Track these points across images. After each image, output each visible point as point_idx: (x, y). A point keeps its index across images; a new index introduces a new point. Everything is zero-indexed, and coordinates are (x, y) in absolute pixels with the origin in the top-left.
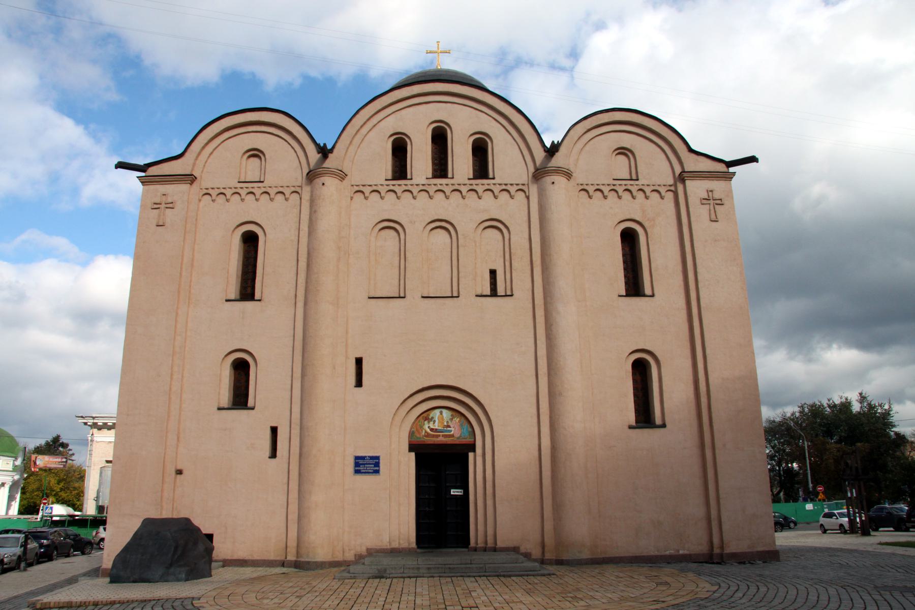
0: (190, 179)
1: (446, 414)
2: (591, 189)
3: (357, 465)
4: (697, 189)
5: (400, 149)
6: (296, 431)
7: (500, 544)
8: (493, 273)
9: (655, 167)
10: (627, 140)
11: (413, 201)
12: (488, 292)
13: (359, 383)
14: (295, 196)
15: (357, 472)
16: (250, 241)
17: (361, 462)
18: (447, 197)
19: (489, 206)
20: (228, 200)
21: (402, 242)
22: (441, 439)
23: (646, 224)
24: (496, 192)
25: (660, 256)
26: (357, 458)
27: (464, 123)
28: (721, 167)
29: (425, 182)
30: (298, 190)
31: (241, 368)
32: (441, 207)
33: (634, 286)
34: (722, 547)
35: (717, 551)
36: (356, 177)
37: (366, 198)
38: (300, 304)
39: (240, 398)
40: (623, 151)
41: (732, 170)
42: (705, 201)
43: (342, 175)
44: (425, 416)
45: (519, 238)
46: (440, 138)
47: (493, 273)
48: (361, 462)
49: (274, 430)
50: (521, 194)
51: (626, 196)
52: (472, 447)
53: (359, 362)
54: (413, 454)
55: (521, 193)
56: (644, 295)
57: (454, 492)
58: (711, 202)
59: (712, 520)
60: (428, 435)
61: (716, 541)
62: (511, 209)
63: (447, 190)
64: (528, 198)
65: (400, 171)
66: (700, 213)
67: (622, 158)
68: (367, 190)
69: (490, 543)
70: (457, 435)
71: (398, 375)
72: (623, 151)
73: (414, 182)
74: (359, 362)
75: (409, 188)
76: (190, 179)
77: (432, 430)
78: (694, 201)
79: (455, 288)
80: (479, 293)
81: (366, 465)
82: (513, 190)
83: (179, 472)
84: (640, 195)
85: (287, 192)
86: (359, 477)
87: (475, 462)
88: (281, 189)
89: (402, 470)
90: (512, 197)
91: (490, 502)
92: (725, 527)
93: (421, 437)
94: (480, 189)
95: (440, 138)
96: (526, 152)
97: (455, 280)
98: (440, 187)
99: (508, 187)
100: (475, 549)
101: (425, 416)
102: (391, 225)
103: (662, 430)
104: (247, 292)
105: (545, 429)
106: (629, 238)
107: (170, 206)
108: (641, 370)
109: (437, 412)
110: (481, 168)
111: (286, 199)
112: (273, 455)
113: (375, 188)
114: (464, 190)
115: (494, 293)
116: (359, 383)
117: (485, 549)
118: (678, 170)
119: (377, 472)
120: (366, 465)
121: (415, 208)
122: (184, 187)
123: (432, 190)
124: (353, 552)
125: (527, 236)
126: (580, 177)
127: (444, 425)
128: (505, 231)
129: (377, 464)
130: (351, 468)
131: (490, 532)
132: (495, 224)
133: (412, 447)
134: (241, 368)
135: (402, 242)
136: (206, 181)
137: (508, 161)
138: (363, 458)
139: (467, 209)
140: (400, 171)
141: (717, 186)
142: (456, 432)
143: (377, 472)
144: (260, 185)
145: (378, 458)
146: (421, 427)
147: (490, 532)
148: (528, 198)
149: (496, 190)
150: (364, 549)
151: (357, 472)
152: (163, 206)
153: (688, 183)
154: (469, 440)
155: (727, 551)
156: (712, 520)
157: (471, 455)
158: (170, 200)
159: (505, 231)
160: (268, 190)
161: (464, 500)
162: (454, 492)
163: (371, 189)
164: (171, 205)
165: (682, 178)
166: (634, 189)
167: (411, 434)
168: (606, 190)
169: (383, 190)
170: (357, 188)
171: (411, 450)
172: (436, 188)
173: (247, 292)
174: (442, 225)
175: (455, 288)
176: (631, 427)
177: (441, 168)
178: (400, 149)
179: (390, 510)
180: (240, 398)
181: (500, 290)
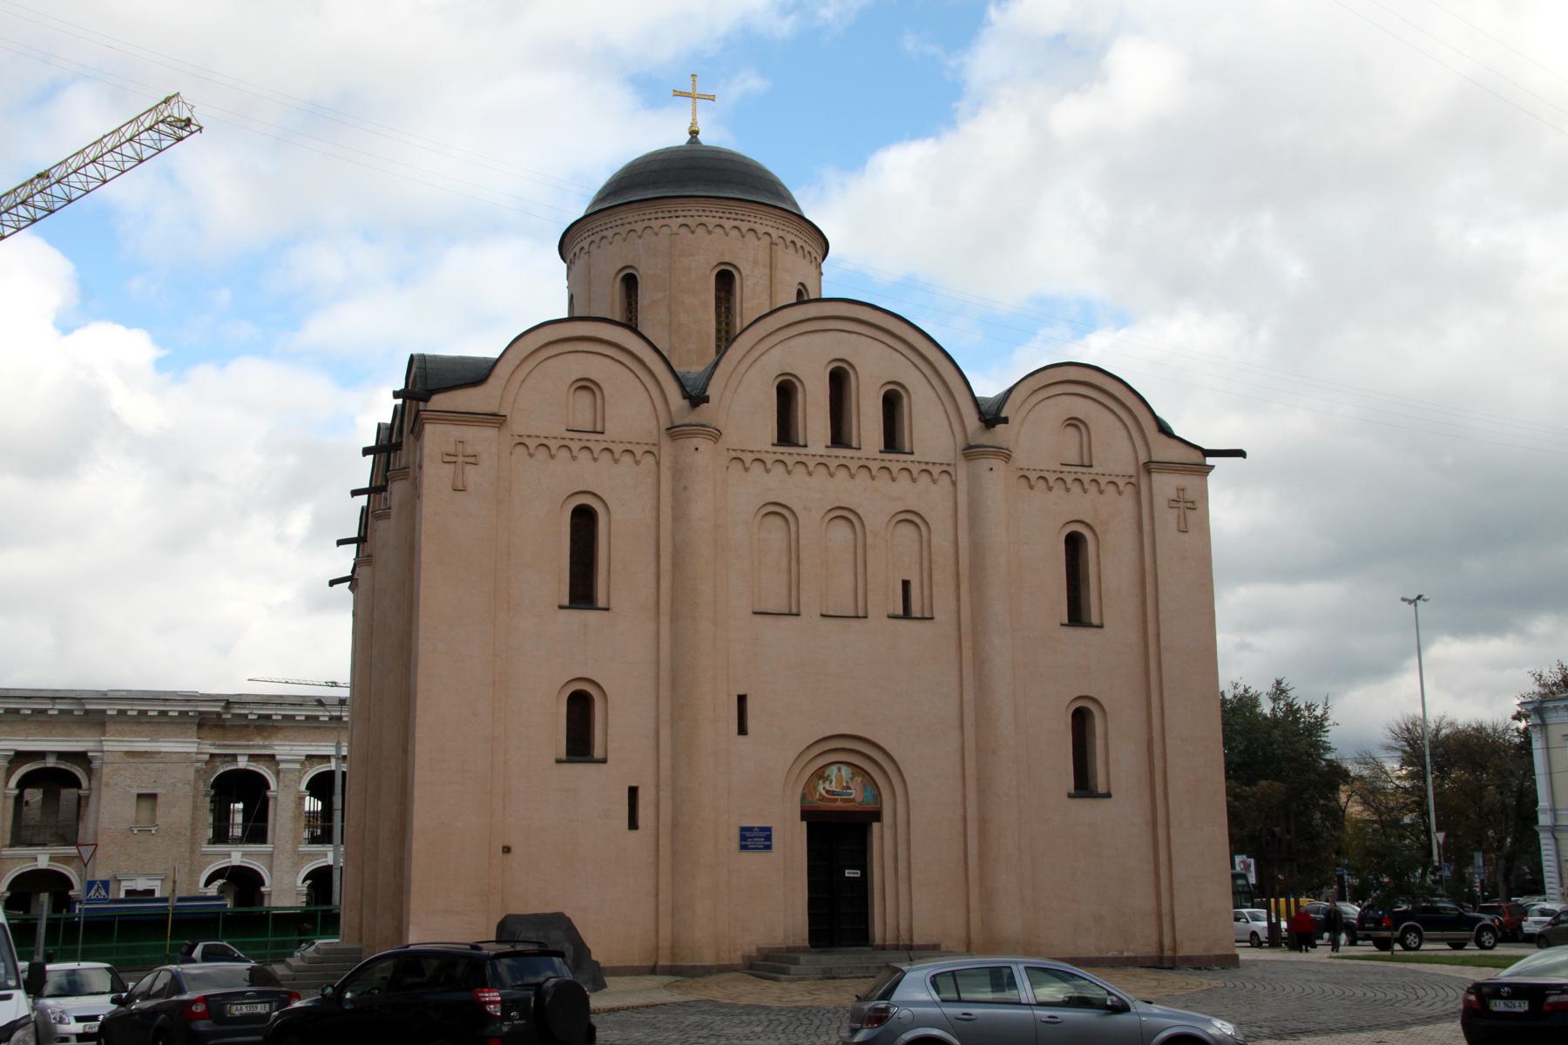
0: (496, 419)
1: (846, 772)
2: (1033, 476)
3: (743, 838)
4: (1165, 485)
5: (786, 392)
6: (665, 794)
7: (917, 941)
8: (906, 584)
9: (1115, 451)
10: (1081, 408)
11: (808, 478)
12: (900, 611)
13: (742, 730)
14: (650, 458)
15: (744, 847)
16: (584, 521)
17: (748, 834)
18: (852, 476)
19: (906, 493)
20: (552, 457)
21: (793, 536)
22: (839, 805)
23: (1097, 530)
24: (915, 473)
25: (1112, 572)
26: (743, 829)
27: (874, 368)
28: (1195, 457)
29: (823, 451)
30: (654, 449)
31: (580, 707)
33: (1077, 615)
34: (1174, 949)
35: (1167, 953)
36: (732, 438)
37: (746, 470)
38: (665, 619)
39: (580, 744)
40: (1074, 423)
41: (1210, 461)
42: (1173, 502)
43: (716, 435)
44: (820, 775)
45: (941, 540)
47: (906, 584)
48: (748, 834)
49: (633, 792)
50: (945, 477)
51: (1076, 488)
52: (876, 815)
53: (742, 699)
54: (802, 828)
55: (945, 476)
56: (1090, 625)
57: (848, 873)
58: (1181, 505)
59: (1163, 916)
60: (823, 799)
61: (1167, 941)
62: (932, 499)
63: (853, 465)
64: (954, 483)
66: (1167, 519)
67: (1071, 430)
68: (748, 458)
69: (904, 940)
70: (859, 800)
72: (1074, 423)
73: (811, 450)
74: (742, 699)
75: (804, 459)
76: (496, 419)
77: (828, 792)
78: (1160, 502)
79: (861, 604)
80: (891, 612)
81: (755, 839)
82: (936, 471)
83: (507, 850)
84: (1093, 488)
85: (638, 451)
86: (746, 855)
87: (880, 835)
88: (629, 447)
90: (934, 481)
91: (903, 887)
92: (1178, 924)
93: (815, 802)
94: (895, 467)
96: (954, 418)
97: (860, 593)
98: (843, 462)
99: (930, 467)
100: (883, 948)
101: (820, 775)
102: (778, 511)
103: (1106, 801)
105: (972, 796)
106: (1074, 544)
107: (473, 459)
108: (1081, 720)
109: (834, 768)
111: (637, 463)
112: (633, 824)
113: (758, 456)
114: (874, 466)
115: (907, 614)
117: (897, 948)
118: (1143, 458)
119: (768, 847)
120: (755, 839)
121: (811, 488)
122: (489, 433)
123: (833, 463)
124: (739, 953)
125: (951, 537)
126: (1021, 458)
128: (918, 521)
129: (769, 838)
130: (736, 843)
131: (903, 925)
132: (911, 518)
133: (806, 815)
134: (580, 707)
135: (793, 536)
136: (518, 425)
137: (930, 429)
138: (750, 829)
139: (877, 495)
140: (786, 434)
141: (1187, 481)
142: (858, 795)
143: (768, 847)
144: (598, 437)
145: (769, 829)
146: (815, 788)
147: (903, 925)
148: (954, 483)
149: (915, 469)
150: (754, 948)
151: (744, 847)
152: (460, 459)
153: (1155, 476)
154: (871, 807)
155: (1181, 953)
156: (1163, 916)
157: (876, 826)
158: (470, 451)
159: (918, 521)
160: (612, 446)
161: (863, 885)
162: (848, 873)
163: (754, 456)
164: (472, 460)
165: (1149, 467)
166: (1086, 479)
167: (803, 797)
168: (1051, 478)
169: (769, 459)
170: (734, 454)
171: (803, 819)
172: (838, 462)
173: (582, 592)
174: (844, 514)
175: (861, 604)
176: (1070, 796)
178: (786, 392)
179: (777, 898)
180: (580, 744)
181: (916, 609)
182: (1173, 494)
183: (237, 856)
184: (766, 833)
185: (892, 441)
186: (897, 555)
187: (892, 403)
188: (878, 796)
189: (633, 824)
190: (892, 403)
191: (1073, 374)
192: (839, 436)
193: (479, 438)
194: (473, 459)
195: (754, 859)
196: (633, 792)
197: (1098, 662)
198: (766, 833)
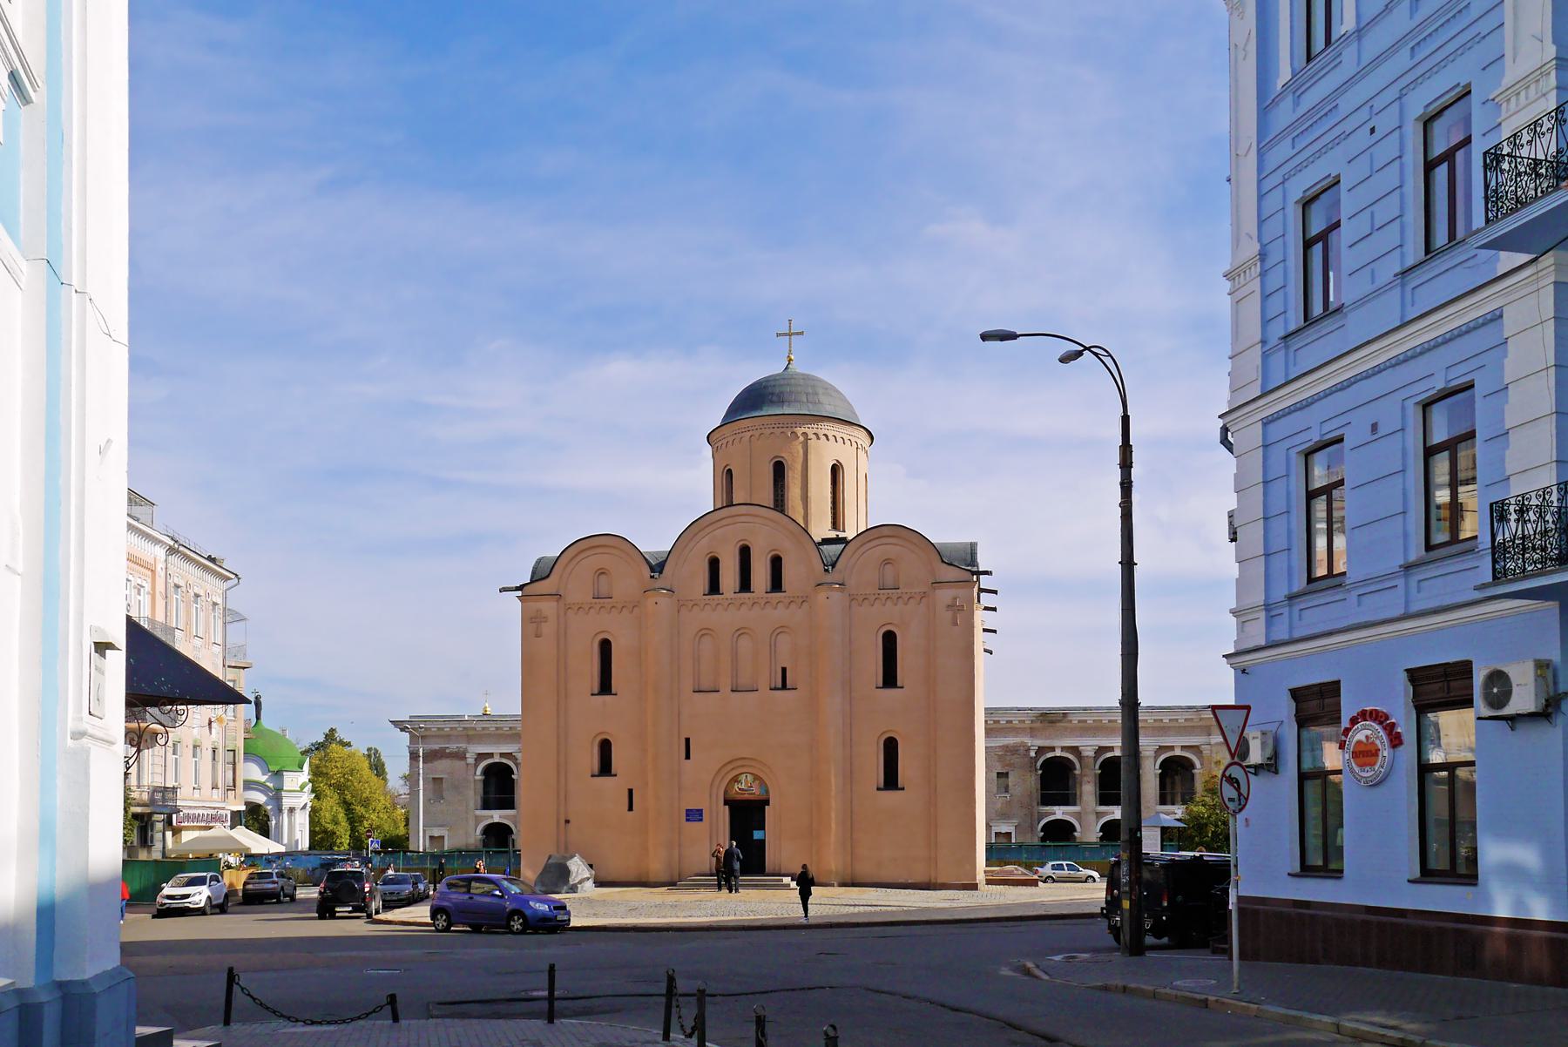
5: (714, 564)
22: (746, 796)
31: (605, 747)
39: (605, 768)
44: (735, 780)
46: (745, 552)
52: (767, 802)
65: (714, 587)
74: (688, 740)
76: (557, 596)
81: (694, 815)
95: (745, 552)
104: (605, 687)
107: (545, 619)
110: (776, 584)
112: (631, 808)
115: (784, 687)
116: (688, 757)
120: (694, 815)
127: (746, 787)
133: (726, 802)
134: (605, 747)
140: (714, 587)
141: (960, 592)
177: (745, 585)
178: (714, 564)
180: (605, 768)
182: (948, 601)
183: (497, 816)
184: (700, 812)
185: (776, 584)
187: (776, 563)
188: (767, 792)
189: (631, 808)
190: (776, 563)
191: (885, 531)
192: (745, 585)
193: (548, 607)
194: (545, 619)
195: (694, 826)
196: (631, 791)
197: (891, 712)
198: (700, 812)
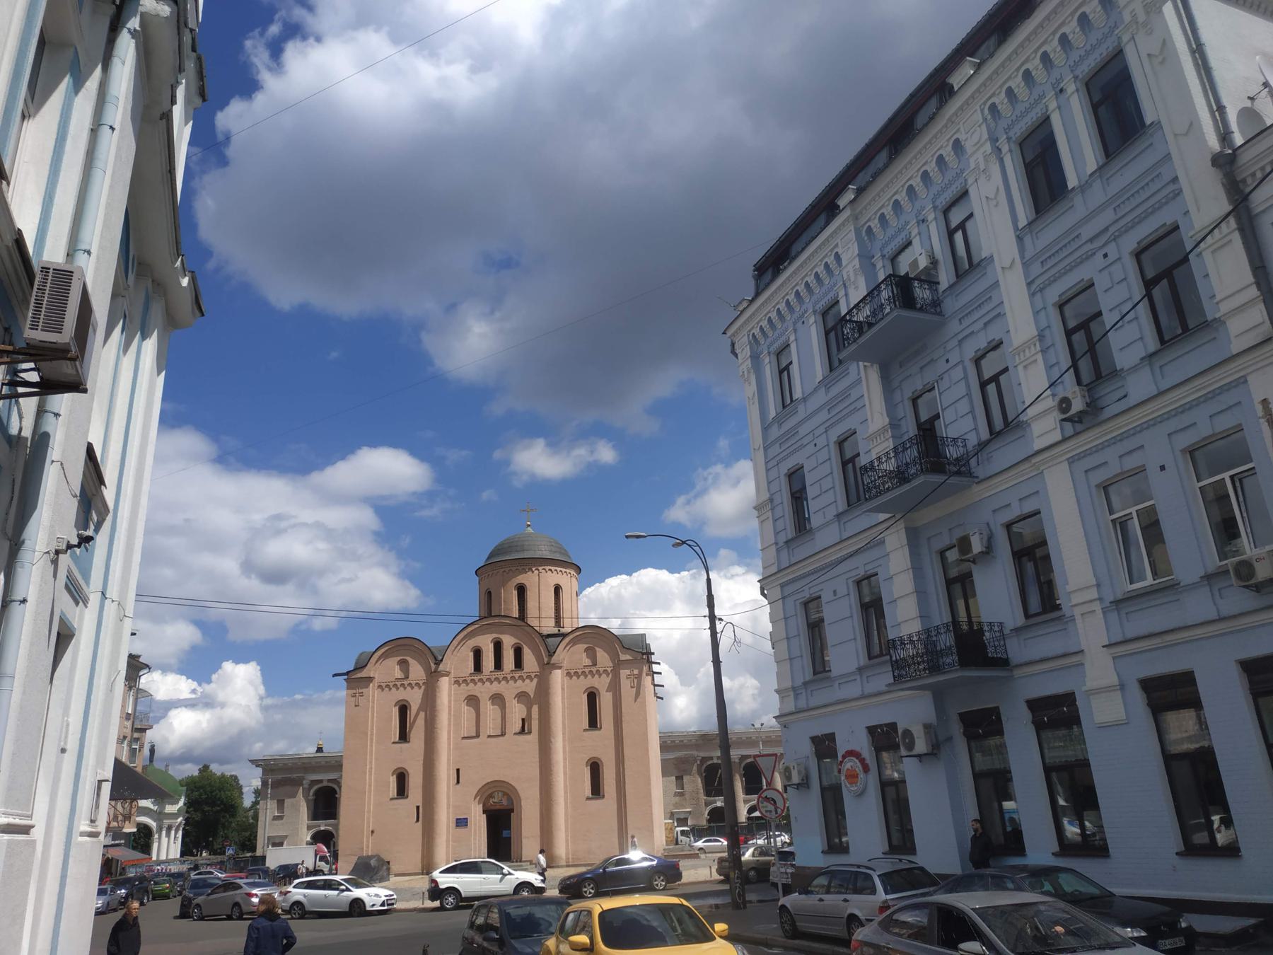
5: (478, 653)
31: (402, 778)
32: (495, 688)
39: (402, 791)
46: (498, 646)
52: (512, 810)
65: (478, 667)
71: (477, 778)
89: (479, 822)
95: (498, 646)
101: (491, 796)
110: (519, 663)
121: (484, 691)
127: (499, 801)
134: (402, 778)
139: (509, 690)
140: (478, 667)
142: (505, 802)
149: (525, 676)
176: (588, 798)
177: (498, 665)
178: (478, 653)
180: (402, 791)
185: (519, 663)
186: (516, 712)
192: (498, 665)
